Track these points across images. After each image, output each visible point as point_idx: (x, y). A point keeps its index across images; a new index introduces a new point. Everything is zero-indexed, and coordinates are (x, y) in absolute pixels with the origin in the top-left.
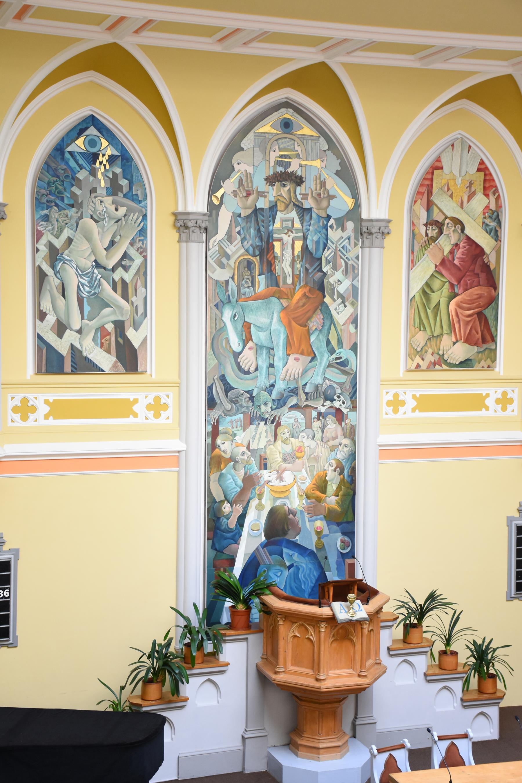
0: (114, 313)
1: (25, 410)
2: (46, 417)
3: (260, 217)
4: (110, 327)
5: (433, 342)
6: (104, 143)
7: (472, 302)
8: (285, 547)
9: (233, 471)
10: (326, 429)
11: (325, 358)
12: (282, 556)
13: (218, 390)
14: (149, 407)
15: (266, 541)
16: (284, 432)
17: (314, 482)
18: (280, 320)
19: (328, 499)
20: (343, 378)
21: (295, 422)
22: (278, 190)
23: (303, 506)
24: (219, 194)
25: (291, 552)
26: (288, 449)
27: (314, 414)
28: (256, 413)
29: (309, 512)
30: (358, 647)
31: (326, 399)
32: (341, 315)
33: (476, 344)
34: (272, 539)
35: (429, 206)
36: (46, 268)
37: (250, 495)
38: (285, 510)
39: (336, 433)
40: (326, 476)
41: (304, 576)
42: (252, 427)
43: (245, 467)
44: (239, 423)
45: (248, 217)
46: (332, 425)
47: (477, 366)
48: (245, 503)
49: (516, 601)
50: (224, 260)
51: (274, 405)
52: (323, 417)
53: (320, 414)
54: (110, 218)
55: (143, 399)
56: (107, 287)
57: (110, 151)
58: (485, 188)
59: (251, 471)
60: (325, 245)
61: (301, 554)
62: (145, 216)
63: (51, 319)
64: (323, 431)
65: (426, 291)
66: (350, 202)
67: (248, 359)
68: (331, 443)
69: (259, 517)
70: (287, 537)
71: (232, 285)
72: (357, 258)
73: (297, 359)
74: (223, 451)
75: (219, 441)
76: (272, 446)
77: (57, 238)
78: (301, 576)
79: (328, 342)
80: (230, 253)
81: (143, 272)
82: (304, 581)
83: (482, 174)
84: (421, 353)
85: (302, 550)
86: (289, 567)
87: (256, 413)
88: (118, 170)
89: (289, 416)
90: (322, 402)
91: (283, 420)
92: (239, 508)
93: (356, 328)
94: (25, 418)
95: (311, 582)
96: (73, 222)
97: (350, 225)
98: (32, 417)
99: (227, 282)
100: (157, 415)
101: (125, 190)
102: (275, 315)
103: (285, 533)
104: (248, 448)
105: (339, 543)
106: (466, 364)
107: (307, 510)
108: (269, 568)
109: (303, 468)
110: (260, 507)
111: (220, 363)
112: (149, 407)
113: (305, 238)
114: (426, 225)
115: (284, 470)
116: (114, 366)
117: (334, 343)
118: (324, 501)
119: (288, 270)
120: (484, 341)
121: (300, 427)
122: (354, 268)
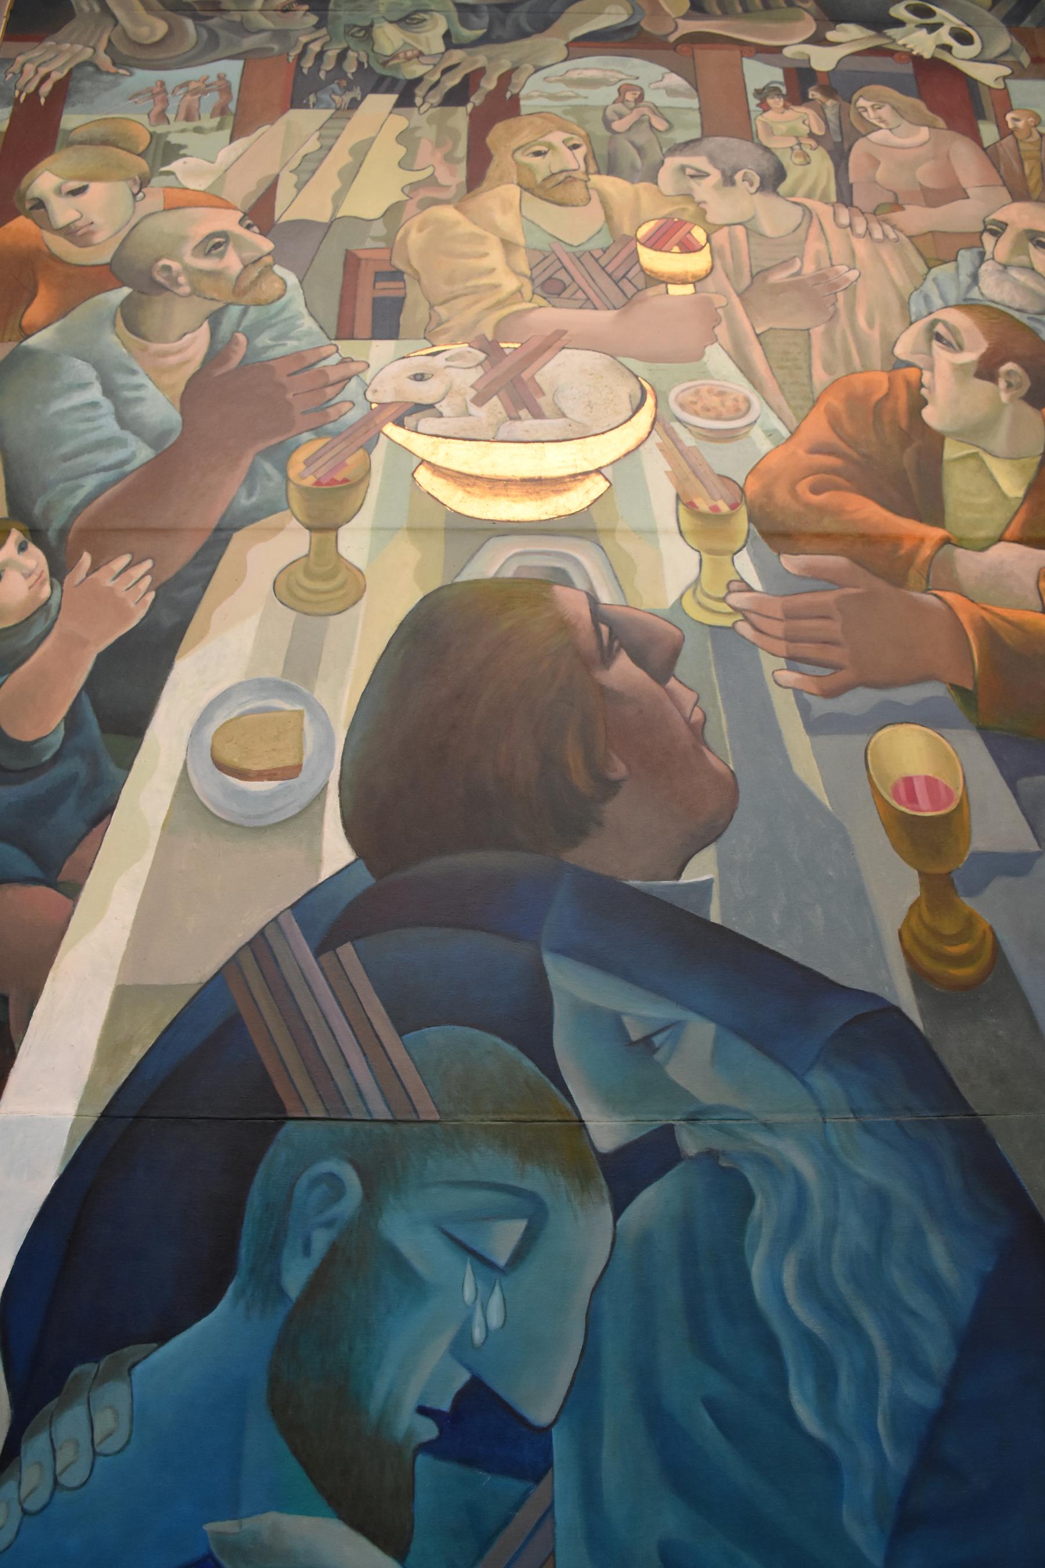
8: (564, 951)
9: (114, 342)
10: (859, 148)
12: (530, 1026)
15: (365, 879)
17: (817, 428)
19: (968, 563)
21: (621, 99)
23: (738, 599)
25: (641, 1011)
26: (576, 226)
28: (342, 56)
29: (809, 650)
34: (435, 866)
37: (231, 491)
38: (564, 625)
39: (947, 170)
40: (925, 403)
41: (811, 1279)
42: (306, 121)
43: (215, 319)
44: (212, 99)
46: (898, 136)
48: (182, 552)
51: (465, 23)
52: (829, 91)
53: (801, 82)
59: (263, 340)
61: (762, 1040)
64: (840, 157)
68: (917, 218)
69: (302, 665)
70: (593, 855)
74: (68, 232)
76: (448, 213)
78: (772, 1274)
82: (808, 1338)
85: (769, 994)
86: (625, 1174)
87: (342, 56)
89: (574, 75)
90: (808, 27)
92: (121, 587)
95: (909, 1358)
107: (778, 628)
108: (382, 1170)
109: (715, 339)
110: (319, 589)
115: (553, 342)
118: (938, 575)
121: (659, 124)
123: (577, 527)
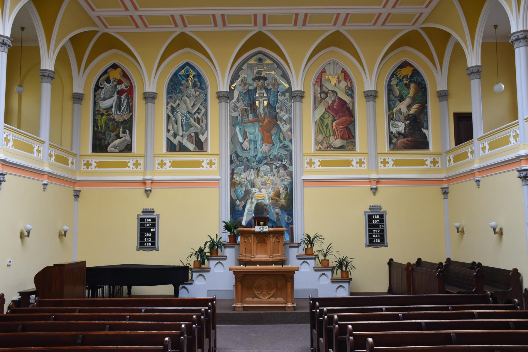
0: (194, 129)
1: (162, 164)
2: (170, 167)
3: (250, 93)
4: (193, 134)
5: (326, 139)
6: (191, 71)
7: (343, 123)
11: (279, 145)
13: (234, 157)
14: (208, 164)
16: (262, 174)
18: (259, 131)
20: (286, 153)
22: (257, 83)
24: (234, 85)
26: (263, 180)
27: (274, 166)
30: (269, 245)
31: (279, 161)
32: (285, 128)
33: (346, 139)
35: (321, 86)
36: (170, 114)
37: (247, 198)
42: (248, 171)
45: (245, 93)
46: (282, 171)
47: (347, 149)
49: (370, 247)
50: (236, 109)
53: (277, 166)
54: (193, 96)
55: (205, 161)
56: (192, 120)
57: (193, 74)
58: (345, 79)
60: (277, 102)
62: (206, 95)
63: (172, 132)
65: (322, 119)
66: (287, 86)
67: (246, 145)
68: (282, 178)
69: (251, 207)
71: (239, 118)
72: (291, 106)
73: (266, 145)
75: (234, 177)
77: (174, 103)
79: (279, 139)
80: (238, 105)
81: (205, 114)
83: (343, 74)
84: (321, 143)
88: (196, 80)
91: (261, 169)
93: (291, 133)
94: (162, 167)
96: (180, 98)
97: (287, 94)
98: (164, 167)
99: (237, 117)
100: (211, 167)
101: (199, 86)
102: (257, 129)
103: (263, 213)
104: (247, 179)
105: (286, 219)
106: (342, 148)
110: (252, 203)
111: (235, 147)
112: (208, 164)
113: (268, 100)
114: (320, 93)
115: (262, 188)
116: (195, 149)
117: (282, 139)
118: (280, 201)
119: (262, 112)
120: (349, 138)
122: (289, 110)
123: (263, 199)
